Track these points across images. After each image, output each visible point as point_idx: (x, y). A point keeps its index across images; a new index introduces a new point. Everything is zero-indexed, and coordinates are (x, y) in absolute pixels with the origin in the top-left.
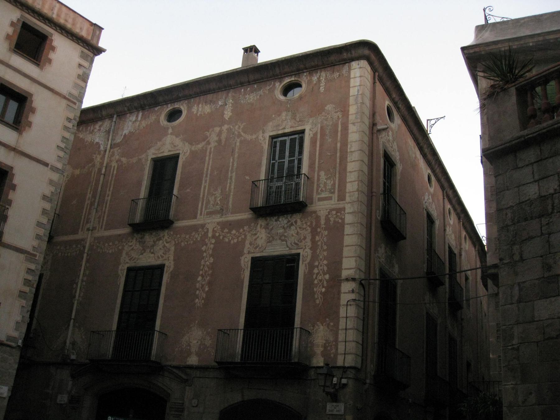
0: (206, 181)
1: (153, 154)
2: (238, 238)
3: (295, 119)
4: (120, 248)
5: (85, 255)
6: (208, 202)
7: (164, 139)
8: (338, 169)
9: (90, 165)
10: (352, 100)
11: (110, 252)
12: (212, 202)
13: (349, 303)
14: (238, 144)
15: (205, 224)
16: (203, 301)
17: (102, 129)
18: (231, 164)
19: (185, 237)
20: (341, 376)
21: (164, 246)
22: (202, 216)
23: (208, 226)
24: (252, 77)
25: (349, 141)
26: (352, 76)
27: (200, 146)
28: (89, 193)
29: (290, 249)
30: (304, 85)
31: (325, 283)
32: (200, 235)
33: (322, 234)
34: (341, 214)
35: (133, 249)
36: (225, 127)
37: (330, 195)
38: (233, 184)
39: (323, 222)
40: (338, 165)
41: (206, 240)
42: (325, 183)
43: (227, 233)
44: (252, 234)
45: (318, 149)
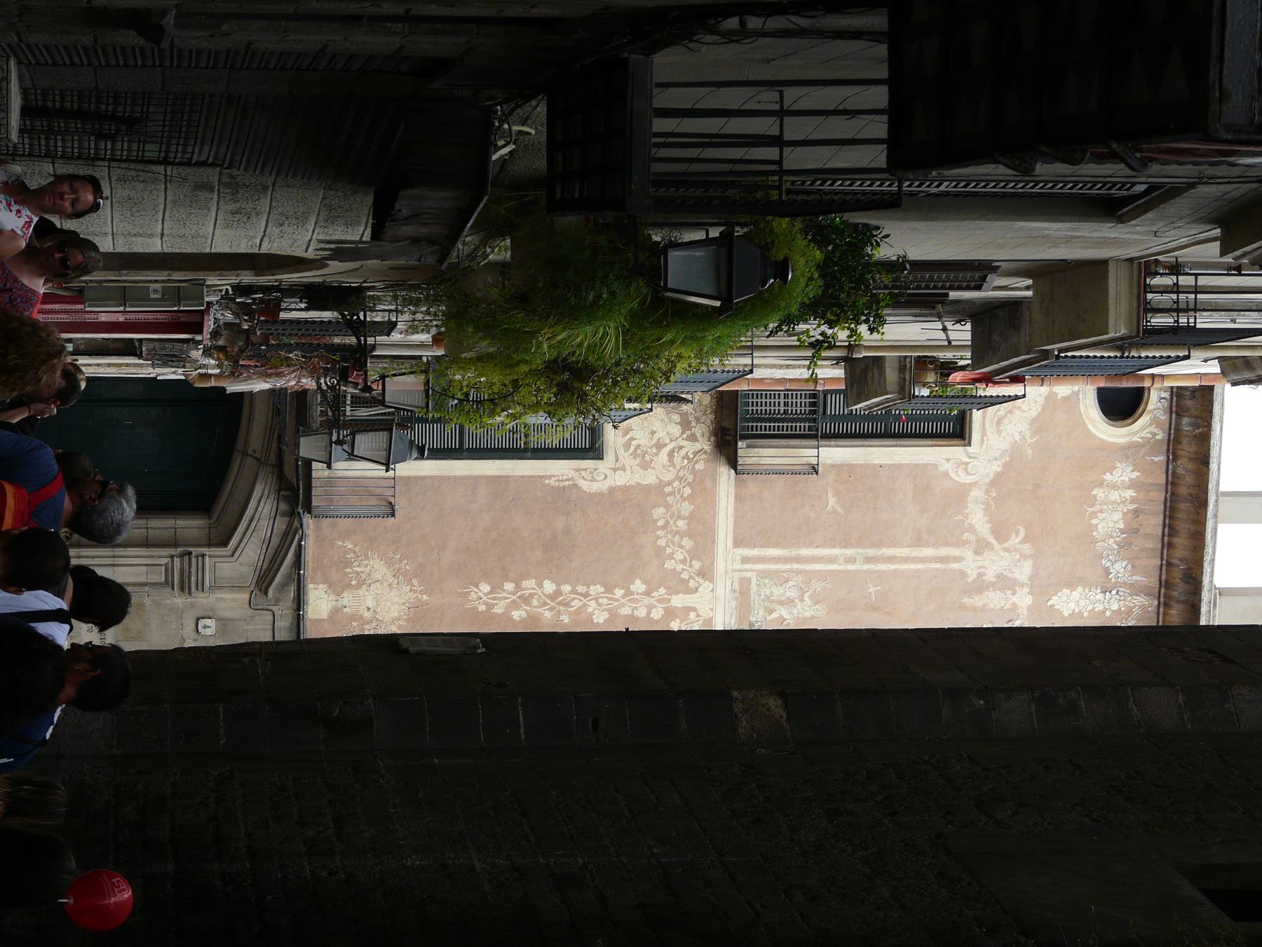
0: (852, 560)
6: (780, 579)
12: (778, 591)
15: (711, 580)
16: (482, 608)
19: (679, 517)
27: (978, 519)
32: (679, 567)
41: (662, 591)
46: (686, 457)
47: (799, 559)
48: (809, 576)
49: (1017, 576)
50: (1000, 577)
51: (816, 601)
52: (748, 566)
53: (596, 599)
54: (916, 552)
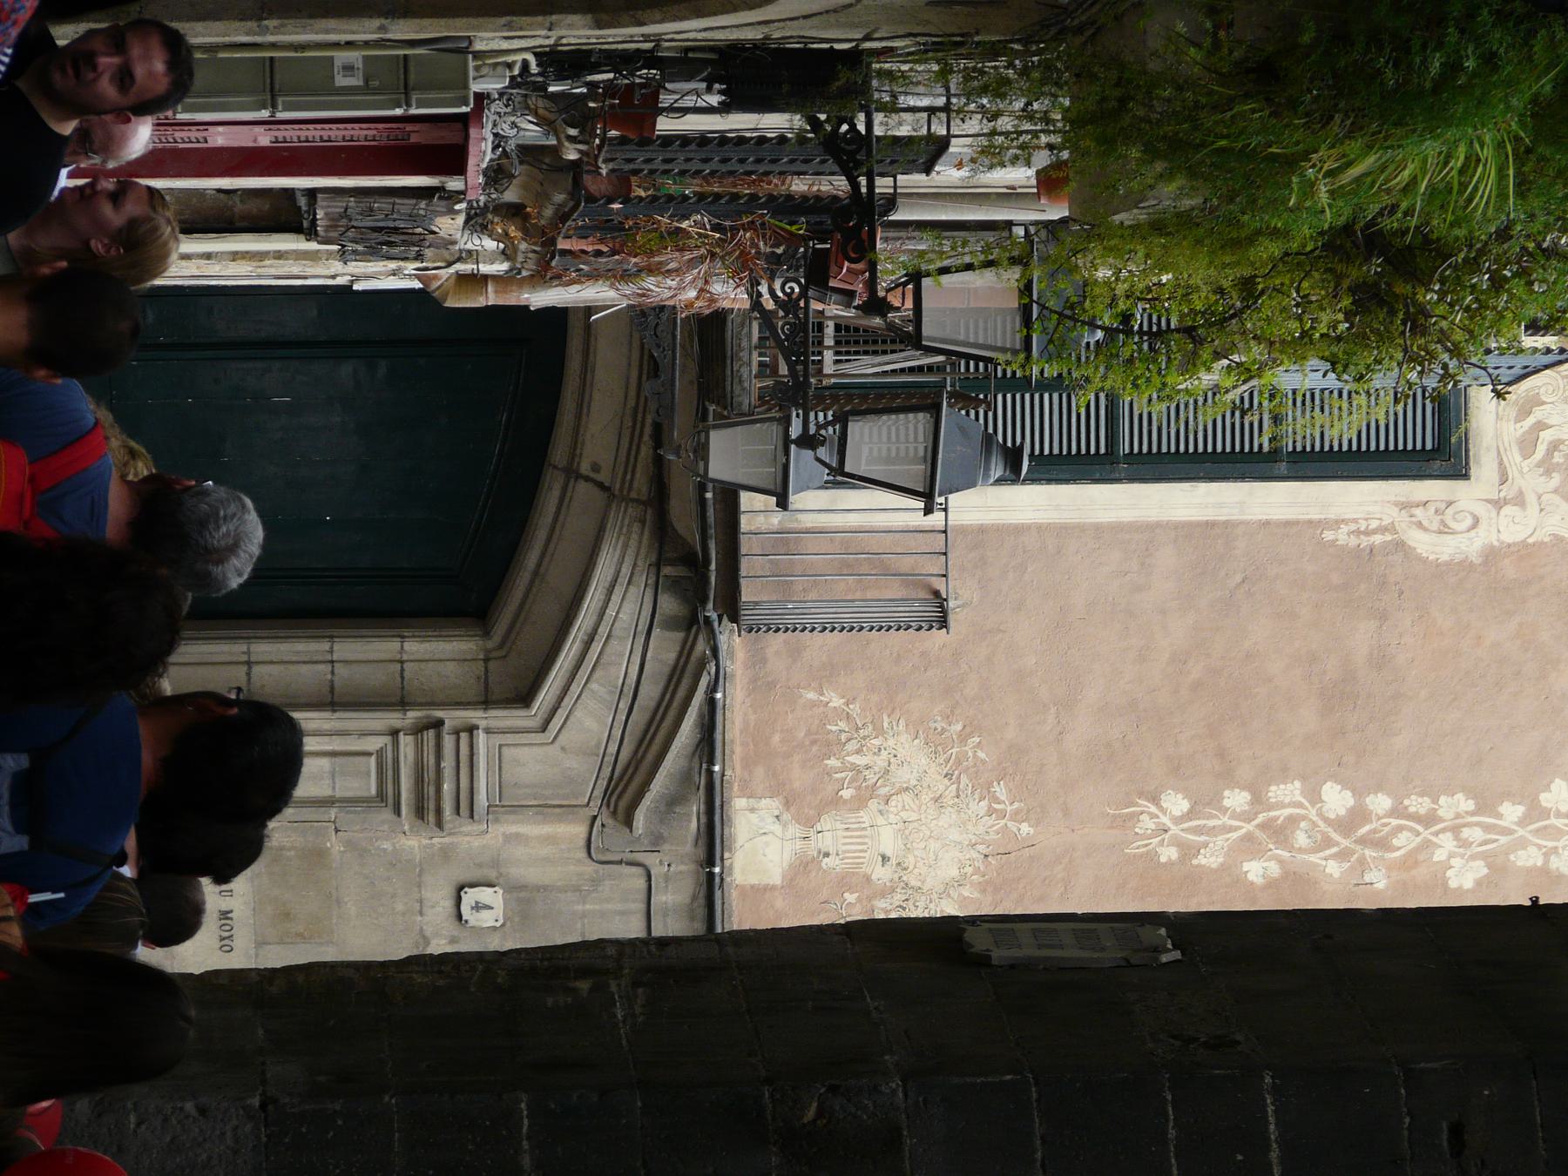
16: (1169, 854)
53: (1455, 830)
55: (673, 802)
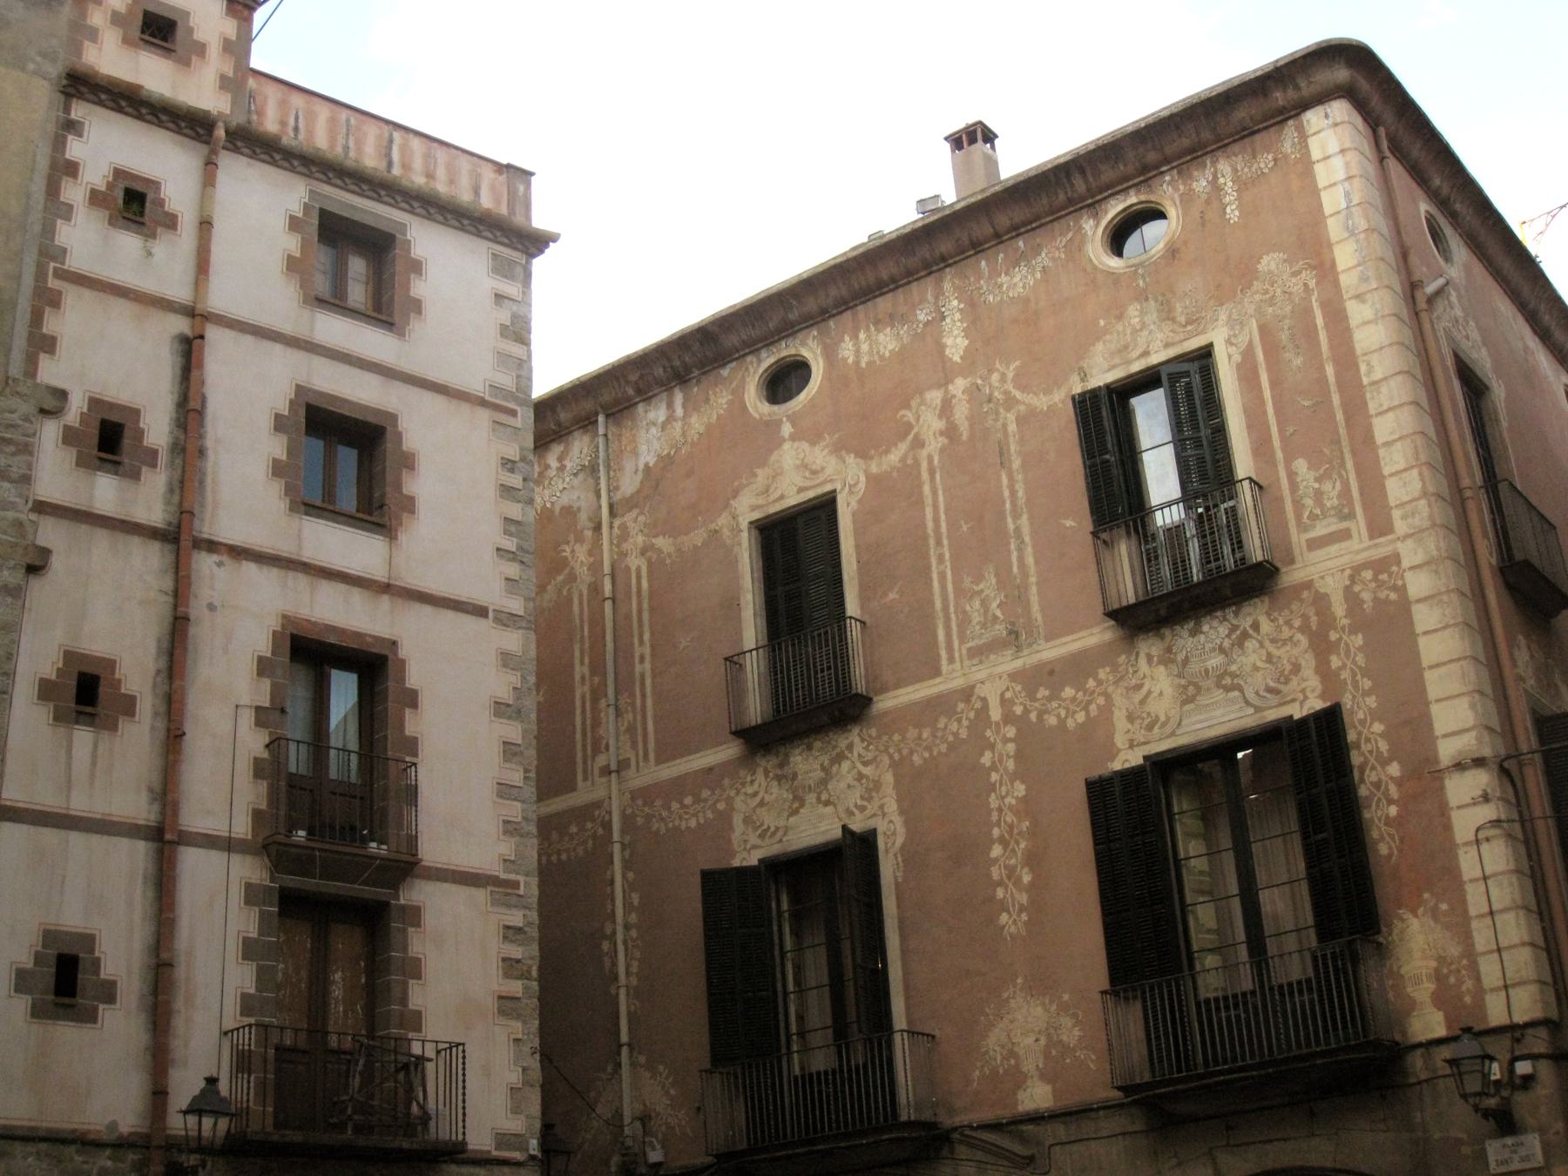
0: (941, 559)
1: (754, 508)
2: (1086, 709)
3: (1173, 320)
4: (721, 806)
5: (617, 848)
6: (965, 621)
7: (773, 458)
8: (1345, 443)
9: (560, 578)
10: (1334, 228)
11: (693, 823)
12: (976, 618)
13: (1481, 836)
14: (1012, 428)
15: (973, 687)
16: (1024, 917)
17: (569, 464)
18: (1006, 493)
19: (920, 738)
20: (1508, 1056)
21: (860, 776)
22: (957, 665)
23: (981, 691)
24: (1003, 220)
25: (1359, 351)
26: (1316, 154)
27: (894, 457)
28: (577, 662)
29: (1258, 709)
30: (1172, 212)
31: (1394, 791)
32: (965, 723)
33: (1347, 644)
34: (1390, 575)
35: (762, 804)
36: (959, 386)
37: (1344, 525)
38: (1029, 549)
39: (1339, 609)
40: (1342, 431)
41: (988, 733)
42: (1318, 495)
43: (1050, 699)
44: (1128, 689)
45: (1267, 394)
46: (866, 748)
47: (945, 608)
48: (959, 591)
49: (939, 402)
50: (940, 417)
51: (979, 578)
52: (957, 655)
53: (1003, 798)
54: (929, 501)
55: (1023, 1139)
